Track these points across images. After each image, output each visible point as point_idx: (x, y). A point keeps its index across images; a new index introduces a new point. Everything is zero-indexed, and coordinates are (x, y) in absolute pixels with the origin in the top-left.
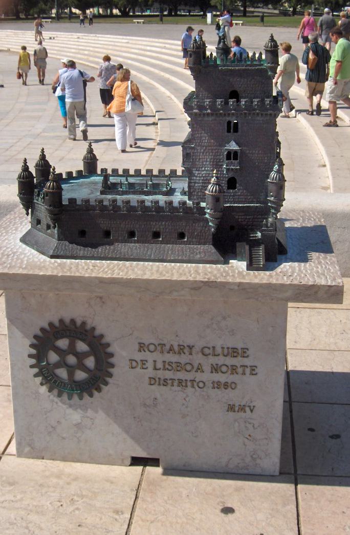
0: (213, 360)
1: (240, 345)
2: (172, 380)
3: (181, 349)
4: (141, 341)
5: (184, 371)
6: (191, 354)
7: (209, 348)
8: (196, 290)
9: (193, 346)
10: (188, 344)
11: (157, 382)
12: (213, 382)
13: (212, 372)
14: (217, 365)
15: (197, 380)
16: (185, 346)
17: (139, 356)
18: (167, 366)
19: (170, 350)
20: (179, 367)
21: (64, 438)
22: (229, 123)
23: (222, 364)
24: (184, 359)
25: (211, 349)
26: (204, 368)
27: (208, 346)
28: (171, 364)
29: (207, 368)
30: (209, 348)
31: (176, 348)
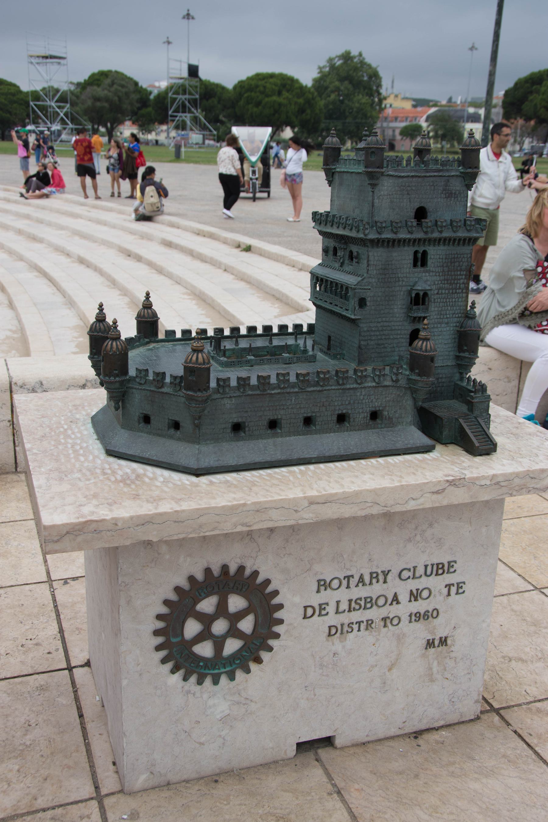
0: (413, 585)
1: (445, 560)
2: (359, 623)
3: (374, 576)
4: (322, 577)
5: (375, 607)
6: (385, 582)
7: (409, 570)
8: (439, 493)
9: (389, 571)
10: (384, 569)
11: (339, 631)
12: (410, 616)
13: (410, 601)
14: (417, 590)
15: (391, 616)
16: (379, 572)
17: (315, 600)
18: (354, 605)
19: (359, 582)
20: (369, 602)
21: (202, 744)
22: (416, 253)
23: (424, 587)
24: (376, 590)
25: (412, 570)
26: (400, 598)
27: (408, 567)
28: (359, 601)
29: (404, 597)
30: (409, 570)
31: (367, 579)
